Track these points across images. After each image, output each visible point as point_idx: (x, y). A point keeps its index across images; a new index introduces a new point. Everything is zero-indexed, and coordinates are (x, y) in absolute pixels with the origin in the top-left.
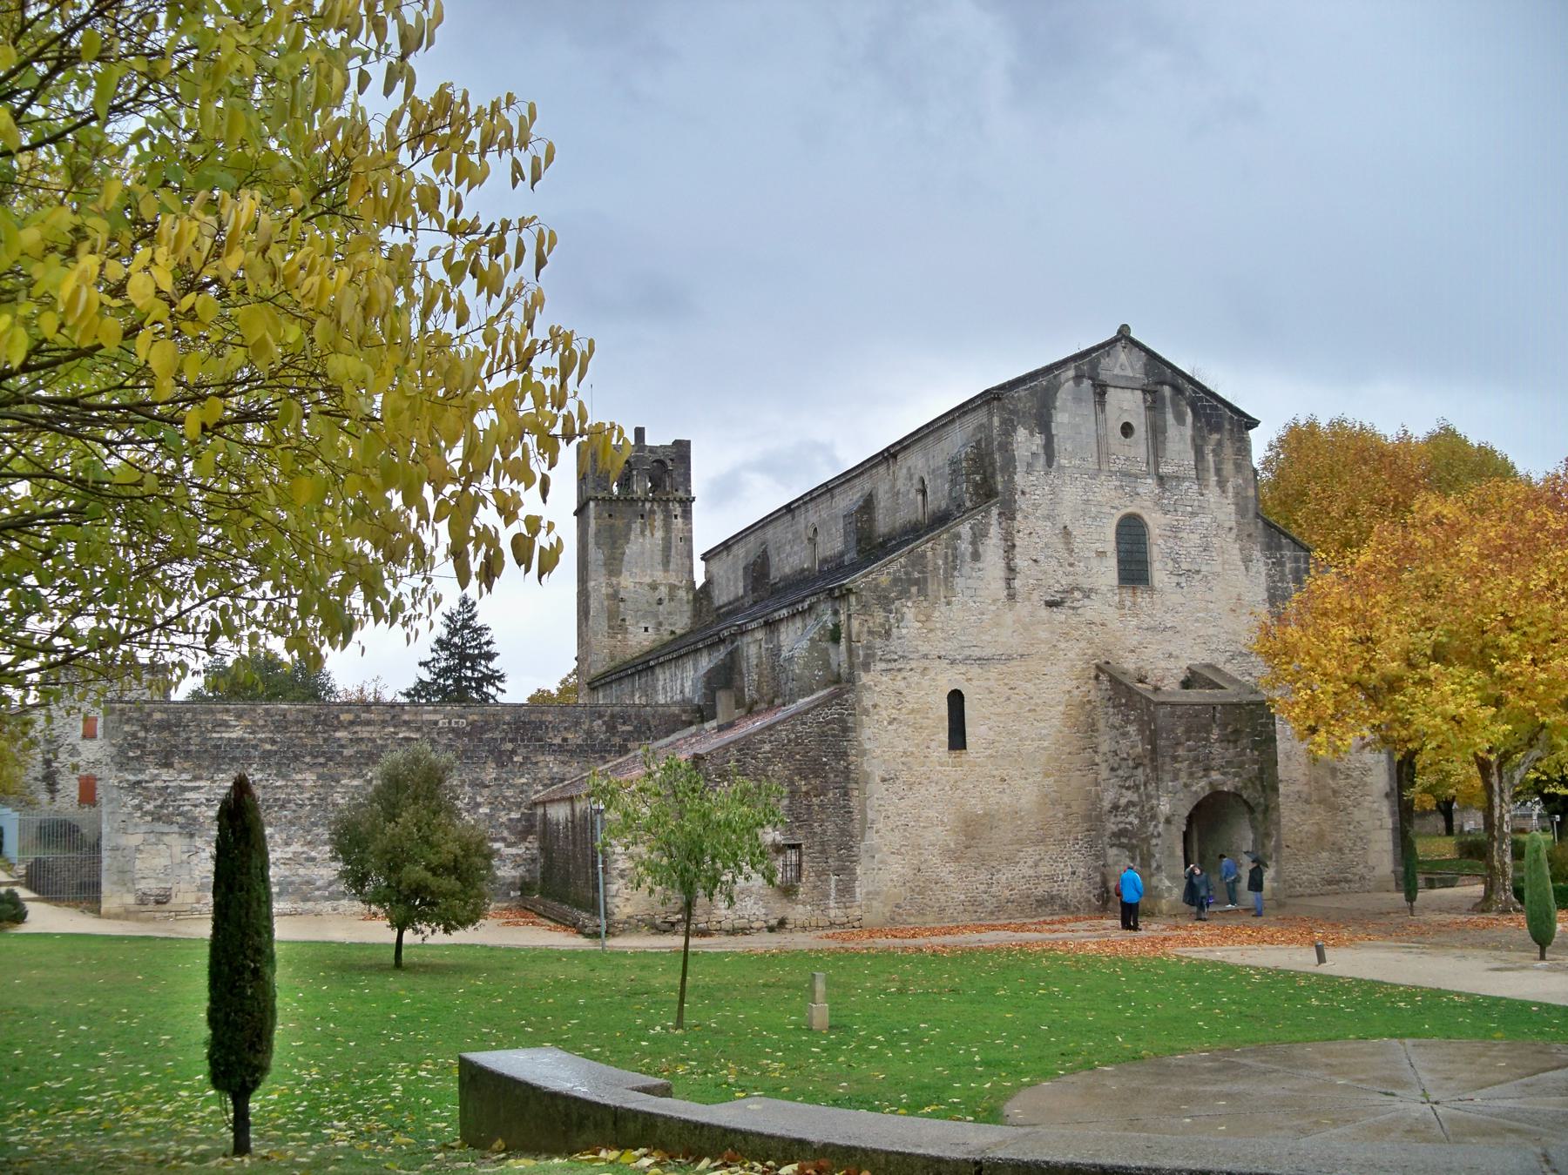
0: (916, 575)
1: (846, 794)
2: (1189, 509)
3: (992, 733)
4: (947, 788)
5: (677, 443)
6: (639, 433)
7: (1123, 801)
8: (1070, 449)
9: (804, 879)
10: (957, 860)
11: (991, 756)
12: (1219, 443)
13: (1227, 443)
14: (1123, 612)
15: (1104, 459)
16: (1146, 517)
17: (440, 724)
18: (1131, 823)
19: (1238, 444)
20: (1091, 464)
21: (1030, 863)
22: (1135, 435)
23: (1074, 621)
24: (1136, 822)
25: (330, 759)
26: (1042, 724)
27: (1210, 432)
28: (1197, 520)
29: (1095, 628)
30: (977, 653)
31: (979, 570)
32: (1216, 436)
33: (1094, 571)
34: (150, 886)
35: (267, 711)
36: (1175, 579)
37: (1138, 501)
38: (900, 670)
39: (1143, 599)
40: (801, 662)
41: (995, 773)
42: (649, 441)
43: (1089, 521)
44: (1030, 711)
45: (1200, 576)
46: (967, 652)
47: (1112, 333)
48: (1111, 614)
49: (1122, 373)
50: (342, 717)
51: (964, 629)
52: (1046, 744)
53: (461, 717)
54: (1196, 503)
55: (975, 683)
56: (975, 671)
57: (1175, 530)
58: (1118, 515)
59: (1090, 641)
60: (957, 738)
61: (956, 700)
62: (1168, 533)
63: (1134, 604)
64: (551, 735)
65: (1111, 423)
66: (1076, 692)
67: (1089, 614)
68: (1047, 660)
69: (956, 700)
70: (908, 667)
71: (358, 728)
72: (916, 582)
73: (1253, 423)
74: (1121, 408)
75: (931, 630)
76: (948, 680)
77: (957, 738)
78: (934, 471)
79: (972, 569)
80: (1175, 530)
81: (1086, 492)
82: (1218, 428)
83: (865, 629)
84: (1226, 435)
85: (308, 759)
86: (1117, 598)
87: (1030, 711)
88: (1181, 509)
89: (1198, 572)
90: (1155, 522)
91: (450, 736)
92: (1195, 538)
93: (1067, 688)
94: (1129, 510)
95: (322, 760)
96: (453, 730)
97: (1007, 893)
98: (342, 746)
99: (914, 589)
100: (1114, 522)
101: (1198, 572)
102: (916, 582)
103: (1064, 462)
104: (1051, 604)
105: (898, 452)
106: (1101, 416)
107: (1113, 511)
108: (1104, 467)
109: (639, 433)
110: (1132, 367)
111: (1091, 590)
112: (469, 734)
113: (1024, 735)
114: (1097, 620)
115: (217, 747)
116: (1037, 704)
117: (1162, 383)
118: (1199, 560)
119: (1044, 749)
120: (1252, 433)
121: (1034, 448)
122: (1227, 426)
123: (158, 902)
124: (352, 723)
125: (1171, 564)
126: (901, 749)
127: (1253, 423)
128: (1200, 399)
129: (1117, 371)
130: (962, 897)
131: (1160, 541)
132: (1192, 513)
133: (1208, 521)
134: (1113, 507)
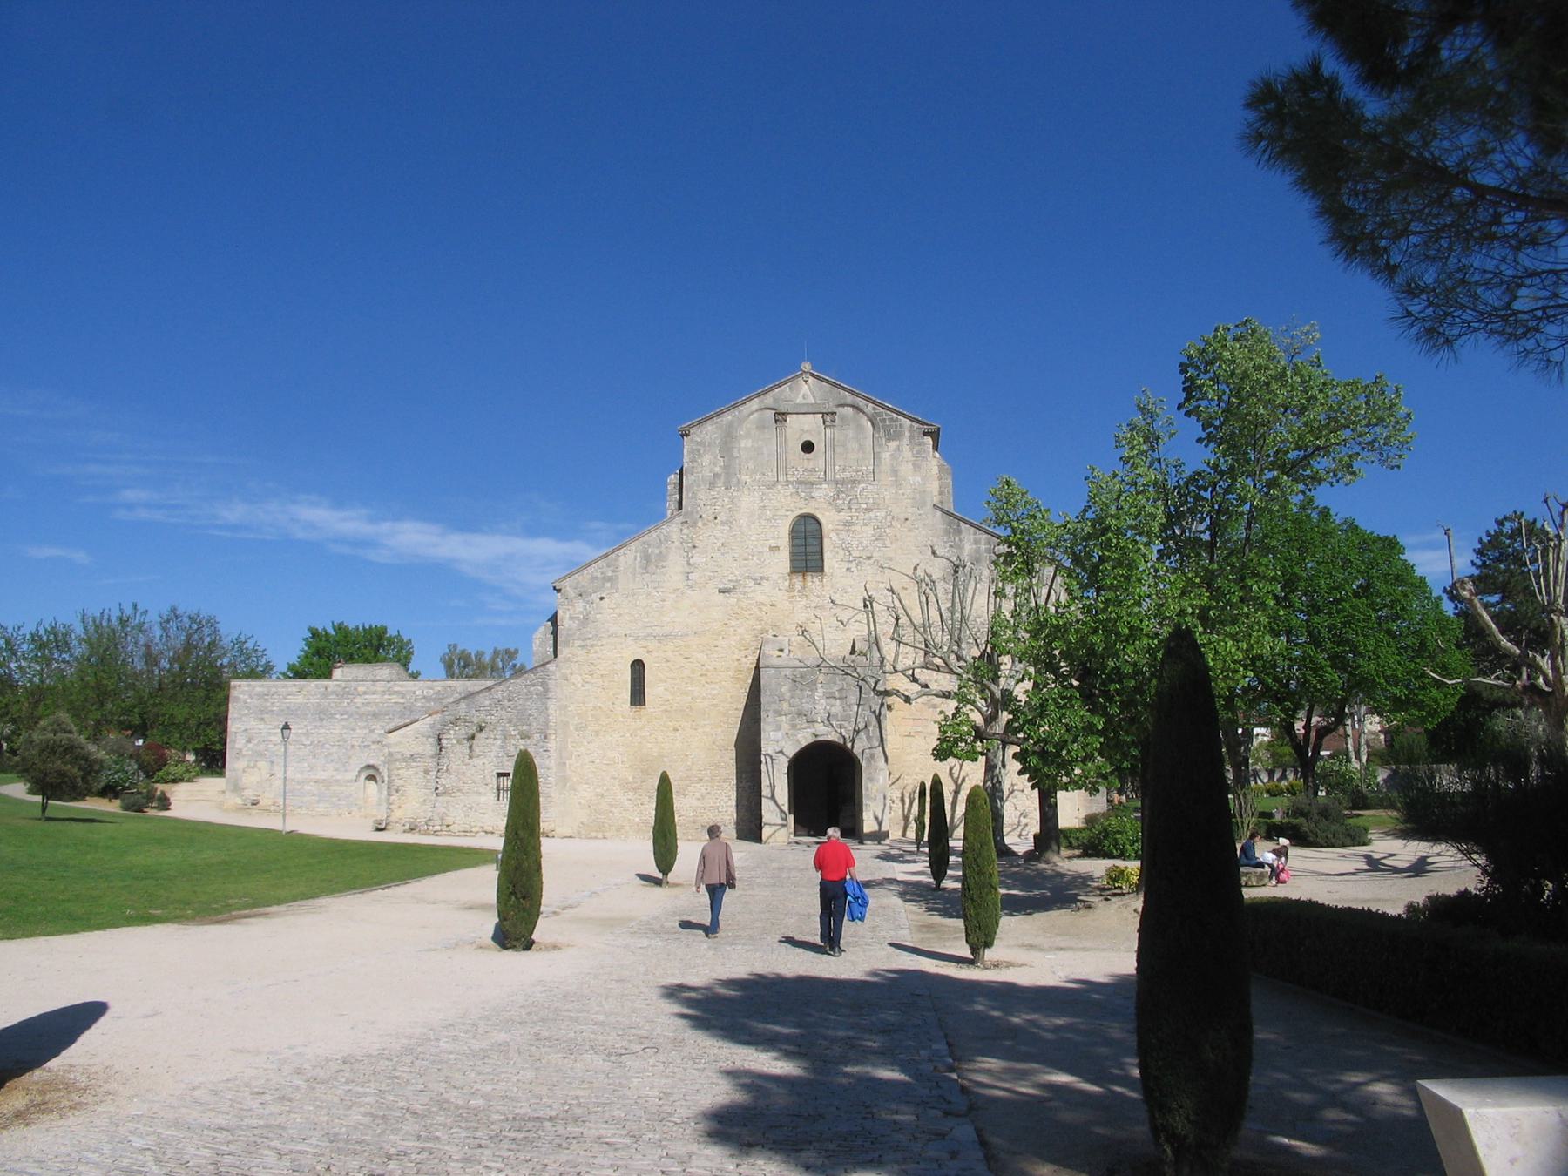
0: (610, 574)
1: (545, 737)
2: (864, 506)
3: (667, 693)
4: (628, 735)
8: (751, 466)
10: (635, 790)
11: (666, 711)
12: (898, 449)
13: (906, 449)
14: (792, 594)
15: (781, 472)
16: (820, 516)
17: (417, 693)
19: (917, 448)
20: (772, 477)
21: (698, 795)
23: (745, 603)
25: (351, 715)
26: (713, 686)
27: (889, 440)
28: (872, 514)
29: (764, 608)
30: (657, 630)
31: (663, 567)
32: (893, 444)
33: (767, 562)
34: (249, 794)
35: (316, 686)
36: (846, 565)
37: (813, 503)
38: (592, 646)
39: (813, 582)
43: (764, 523)
44: (701, 675)
45: (871, 561)
46: (649, 630)
48: (780, 597)
49: (804, 402)
50: (359, 689)
51: (647, 613)
52: (715, 702)
53: (432, 689)
54: (871, 501)
55: (655, 654)
56: (653, 645)
57: (848, 525)
58: (792, 516)
59: (759, 620)
60: (638, 695)
61: (638, 667)
62: (842, 528)
63: (804, 587)
65: (790, 444)
66: (744, 660)
67: (760, 598)
68: (719, 634)
69: (638, 667)
70: (600, 643)
71: (367, 697)
72: (610, 579)
74: (802, 430)
75: (620, 615)
77: (638, 695)
79: (657, 567)
80: (848, 525)
81: (762, 501)
82: (897, 436)
83: (568, 616)
84: (906, 441)
85: (338, 716)
86: (787, 584)
87: (701, 675)
88: (854, 507)
89: (869, 558)
90: (829, 520)
91: (423, 700)
92: (869, 531)
93: (736, 657)
95: (345, 717)
96: (424, 697)
98: (358, 708)
99: (608, 585)
101: (869, 558)
102: (610, 579)
103: (745, 478)
104: (722, 591)
106: (781, 439)
107: (788, 513)
108: (782, 478)
110: (814, 397)
111: (761, 578)
112: (434, 700)
113: (696, 694)
114: (767, 602)
115: (288, 708)
116: (707, 670)
117: (843, 405)
118: (871, 548)
121: (717, 469)
122: (907, 434)
123: (253, 804)
124: (365, 693)
125: (842, 552)
126: (591, 705)
128: (880, 414)
129: (799, 400)
130: (637, 819)
131: (833, 535)
132: (866, 509)
133: (883, 514)
134: (787, 510)
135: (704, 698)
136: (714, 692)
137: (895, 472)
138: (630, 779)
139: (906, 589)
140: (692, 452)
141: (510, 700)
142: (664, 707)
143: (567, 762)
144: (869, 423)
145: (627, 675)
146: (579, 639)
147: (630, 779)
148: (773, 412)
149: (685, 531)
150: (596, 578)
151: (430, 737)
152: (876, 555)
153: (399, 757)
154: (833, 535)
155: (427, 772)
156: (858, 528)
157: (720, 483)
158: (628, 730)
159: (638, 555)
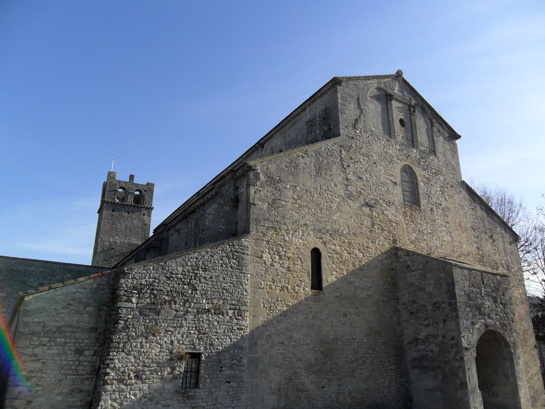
4: (310, 317)
5: (148, 184)
6: (132, 177)
7: (422, 336)
9: (201, 385)
11: (337, 297)
18: (432, 351)
22: (406, 127)
24: (436, 349)
39: (416, 214)
40: (210, 217)
41: (341, 309)
42: (136, 181)
47: (394, 72)
52: (370, 293)
61: (316, 254)
64: (32, 280)
66: (385, 262)
69: (316, 254)
73: (458, 137)
76: (314, 242)
78: (289, 142)
94: (407, 163)
97: (349, 402)
100: (400, 167)
102: (293, 174)
105: (265, 142)
109: (132, 177)
113: (357, 285)
119: (369, 296)
120: (458, 142)
127: (458, 137)
131: (422, 184)
135: (362, 289)
136: (369, 285)
137: (445, 155)
138: (313, 362)
139: (458, 230)
140: (342, 97)
141: (205, 270)
142: (336, 294)
143: (259, 342)
144: (429, 122)
145: (308, 264)
146: (268, 219)
147: (313, 362)
148: (384, 92)
149: (343, 152)
150: (282, 169)
151: (88, 305)
152: (444, 204)
153: (39, 329)
154: (422, 184)
155: (79, 352)
156: (433, 183)
157: (360, 125)
158: (310, 312)
159: (313, 161)
